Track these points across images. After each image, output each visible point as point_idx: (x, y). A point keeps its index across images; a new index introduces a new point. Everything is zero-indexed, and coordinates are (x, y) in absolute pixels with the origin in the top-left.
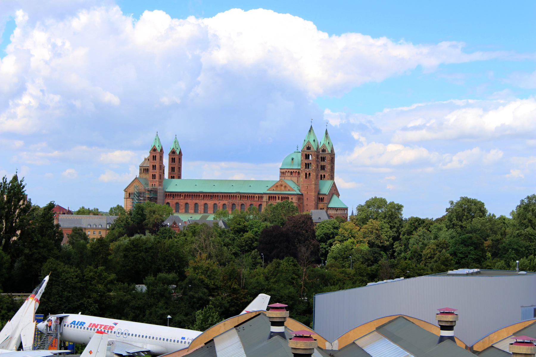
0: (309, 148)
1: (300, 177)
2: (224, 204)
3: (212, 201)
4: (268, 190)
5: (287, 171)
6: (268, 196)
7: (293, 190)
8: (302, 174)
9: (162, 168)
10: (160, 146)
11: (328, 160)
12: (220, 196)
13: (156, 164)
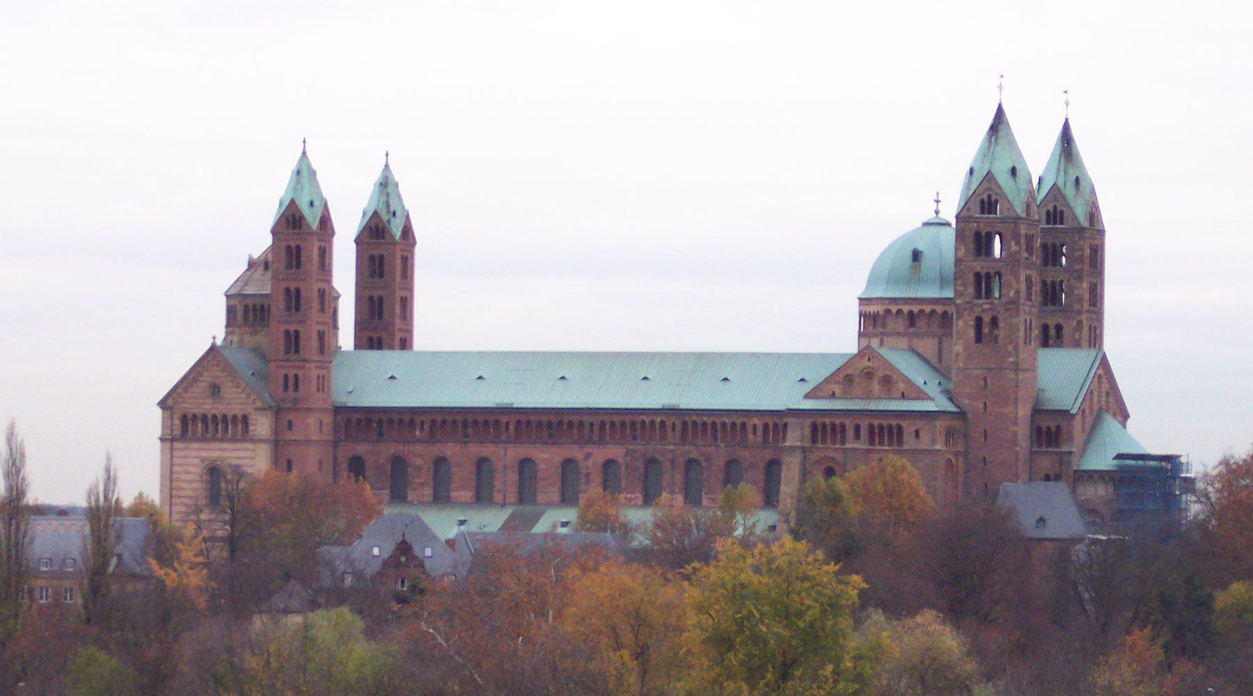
0: (988, 206)
2: (609, 464)
4: (807, 396)
5: (894, 309)
6: (808, 422)
7: (921, 395)
8: (959, 325)
9: (327, 299)
10: (317, 203)
12: (592, 425)
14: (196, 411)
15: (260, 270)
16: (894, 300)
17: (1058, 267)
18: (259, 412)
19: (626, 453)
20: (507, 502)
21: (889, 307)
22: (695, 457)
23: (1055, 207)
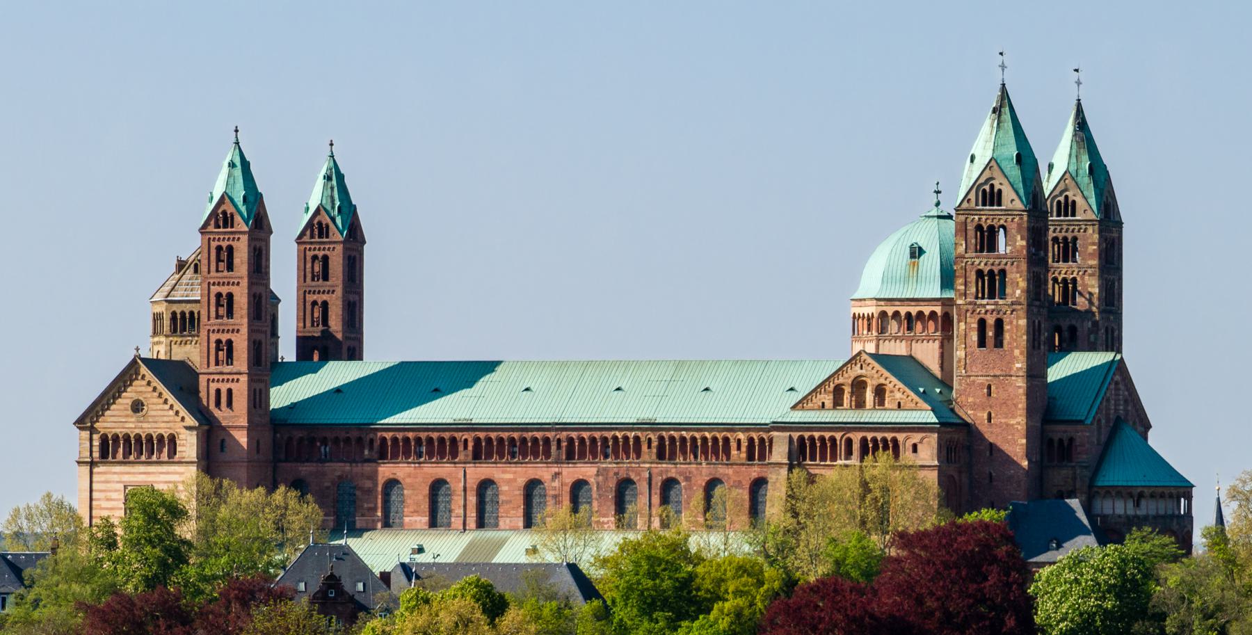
0: (991, 197)
1: (952, 337)
3: (519, 469)
5: (890, 311)
8: (959, 328)
11: (1091, 255)
13: (233, 289)
14: (118, 431)
15: (190, 272)
16: (890, 301)
17: (1070, 263)
18: (188, 432)
19: (598, 471)
20: (467, 528)
21: (884, 308)
22: (674, 475)
23: (1067, 197)
